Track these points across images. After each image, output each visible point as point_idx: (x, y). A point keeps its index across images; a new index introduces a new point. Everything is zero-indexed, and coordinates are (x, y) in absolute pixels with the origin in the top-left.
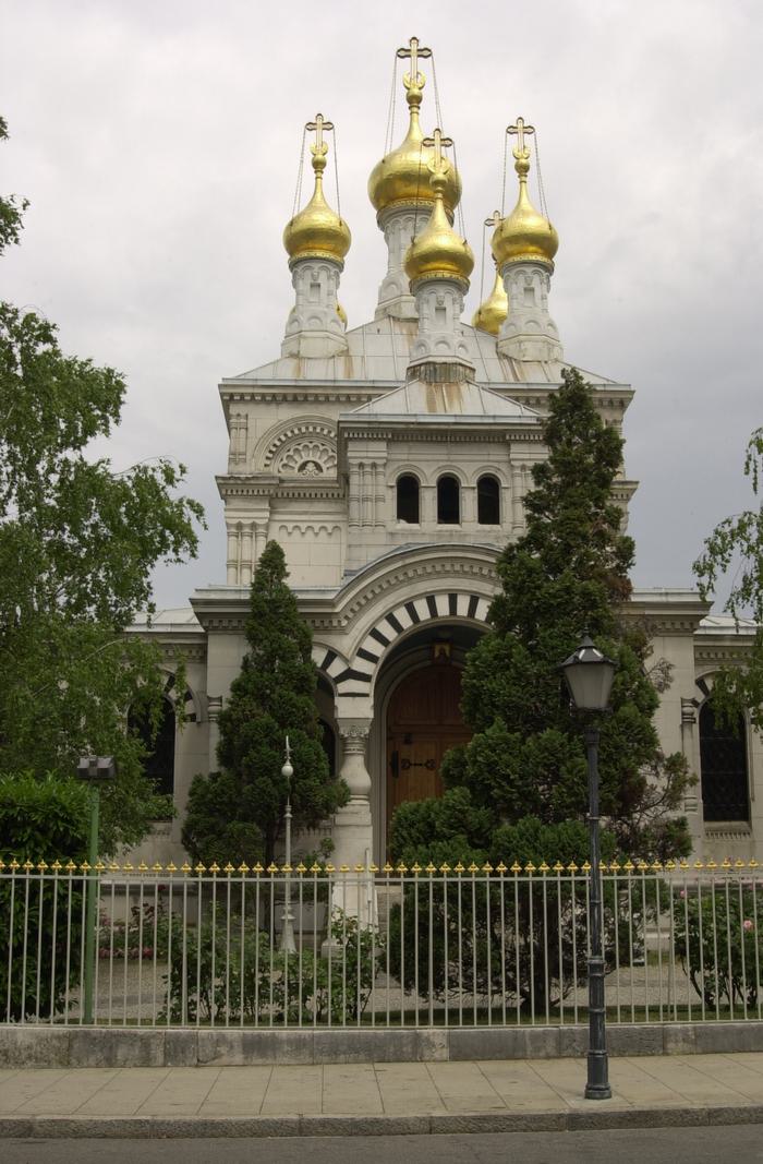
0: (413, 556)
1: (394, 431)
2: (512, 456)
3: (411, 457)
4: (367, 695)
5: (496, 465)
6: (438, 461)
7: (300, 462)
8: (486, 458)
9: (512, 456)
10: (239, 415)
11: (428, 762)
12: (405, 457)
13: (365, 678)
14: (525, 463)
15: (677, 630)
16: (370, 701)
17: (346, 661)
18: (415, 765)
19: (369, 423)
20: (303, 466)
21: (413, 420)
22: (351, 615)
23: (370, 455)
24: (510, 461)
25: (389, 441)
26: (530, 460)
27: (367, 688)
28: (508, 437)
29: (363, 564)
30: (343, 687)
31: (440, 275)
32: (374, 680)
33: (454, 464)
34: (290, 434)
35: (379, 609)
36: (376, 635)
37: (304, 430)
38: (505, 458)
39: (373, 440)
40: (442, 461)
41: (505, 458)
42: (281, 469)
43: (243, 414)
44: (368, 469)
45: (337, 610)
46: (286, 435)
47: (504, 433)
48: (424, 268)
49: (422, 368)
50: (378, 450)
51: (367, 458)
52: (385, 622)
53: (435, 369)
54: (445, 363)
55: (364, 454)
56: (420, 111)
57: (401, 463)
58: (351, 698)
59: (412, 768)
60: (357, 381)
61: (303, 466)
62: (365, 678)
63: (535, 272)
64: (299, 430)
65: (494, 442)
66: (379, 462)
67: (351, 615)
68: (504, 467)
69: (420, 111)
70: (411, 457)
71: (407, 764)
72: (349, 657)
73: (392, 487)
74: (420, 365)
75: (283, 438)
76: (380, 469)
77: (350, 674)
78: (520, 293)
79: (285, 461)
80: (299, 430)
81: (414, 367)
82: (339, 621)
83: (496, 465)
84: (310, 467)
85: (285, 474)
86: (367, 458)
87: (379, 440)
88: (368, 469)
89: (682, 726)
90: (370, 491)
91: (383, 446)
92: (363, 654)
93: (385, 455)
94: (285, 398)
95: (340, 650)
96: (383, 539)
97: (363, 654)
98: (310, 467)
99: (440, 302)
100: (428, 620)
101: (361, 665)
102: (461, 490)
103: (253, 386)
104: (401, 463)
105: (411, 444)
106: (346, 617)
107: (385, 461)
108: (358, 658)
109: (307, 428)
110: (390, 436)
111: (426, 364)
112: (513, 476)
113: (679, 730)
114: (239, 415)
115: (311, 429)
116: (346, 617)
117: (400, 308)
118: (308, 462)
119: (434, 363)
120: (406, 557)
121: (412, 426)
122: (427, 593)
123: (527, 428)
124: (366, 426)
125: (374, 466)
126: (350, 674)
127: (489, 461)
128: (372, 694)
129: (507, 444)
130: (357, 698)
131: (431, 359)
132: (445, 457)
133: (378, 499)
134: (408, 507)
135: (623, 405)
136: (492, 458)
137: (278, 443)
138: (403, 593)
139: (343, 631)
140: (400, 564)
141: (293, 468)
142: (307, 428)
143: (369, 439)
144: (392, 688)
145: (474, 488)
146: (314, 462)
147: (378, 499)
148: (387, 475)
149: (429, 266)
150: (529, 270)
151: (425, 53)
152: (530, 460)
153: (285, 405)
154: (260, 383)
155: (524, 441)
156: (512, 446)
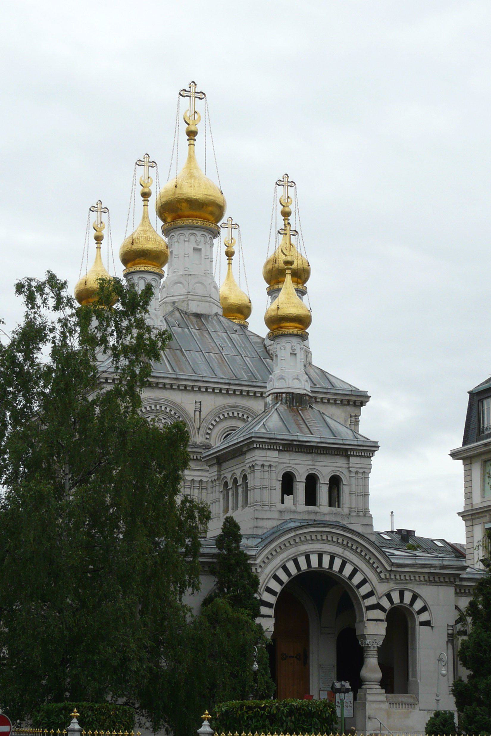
0: (301, 529)
1: (283, 445)
2: (351, 465)
3: (292, 462)
4: (270, 616)
6: (307, 465)
8: (334, 465)
9: (351, 465)
12: (288, 461)
13: (268, 605)
14: (358, 470)
15: (446, 582)
21: (296, 439)
22: (263, 565)
23: (269, 459)
24: (349, 468)
25: (279, 451)
26: (361, 468)
27: (270, 612)
28: (349, 453)
29: (265, 531)
31: (295, 332)
33: (316, 467)
35: (277, 561)
36: (276, 578)
37: (153, 407)
38: (346, 466)
39: (271, 449)
40: (307, 465)
41: (346, 466)
44: (266, 468)
45: (256, 563)
47: (346, 450)
48: (283, 325)
49: (284, 395)
50: (273, 456)
51: (267, 461)
55: (264, 459)
56: (195, 143)
57: (285, 465)
62: (268, 605)
64: (150, 407)
67: (263, 565)
68: (345, 471)
69: (195, 143)
70: (292, 462)
73: (279, 480)
74: (282, 393)
76: (273, 469)
80: (150, 407)
81: (277, 393)
82: (256, 569)
86: (267, 461)
87: (274, 450)
88: (266, 468)
89: (447, 642)
90: (267, 483)
91: (276, 453)
93: (277, 460)
96: (276, 515)
99: (293, 349)
100: (305, 570)
102: (318, 485)
104: (285, 465)
106: (260, 566)
108: (265, 593)
109: (156, 406)
111: (287, 393)
112: (350, 477)
113: (446, 643)
115: (158, 407)
116: (260, 566)
117: (188, 305)
119: (293, 393)
120: (297, 530)
122: (306, 552)
123: (362, 448)
124: (268, 441)
125: (270, 466)
127: (336, 467)
128: (273, 616)
129: (348, 457)
130: (265, 618)
132: (310, 463)
133: (272, 488)
135: (362, 404)
136: (338, 465)
138: (291, 552)
140: (293, 534)
142: (156, 406)
143: (268, 449)
145: (327, 484)
147: (272, 488)
152: (361, 468)
155: (357, 456)
156: (351, 458)
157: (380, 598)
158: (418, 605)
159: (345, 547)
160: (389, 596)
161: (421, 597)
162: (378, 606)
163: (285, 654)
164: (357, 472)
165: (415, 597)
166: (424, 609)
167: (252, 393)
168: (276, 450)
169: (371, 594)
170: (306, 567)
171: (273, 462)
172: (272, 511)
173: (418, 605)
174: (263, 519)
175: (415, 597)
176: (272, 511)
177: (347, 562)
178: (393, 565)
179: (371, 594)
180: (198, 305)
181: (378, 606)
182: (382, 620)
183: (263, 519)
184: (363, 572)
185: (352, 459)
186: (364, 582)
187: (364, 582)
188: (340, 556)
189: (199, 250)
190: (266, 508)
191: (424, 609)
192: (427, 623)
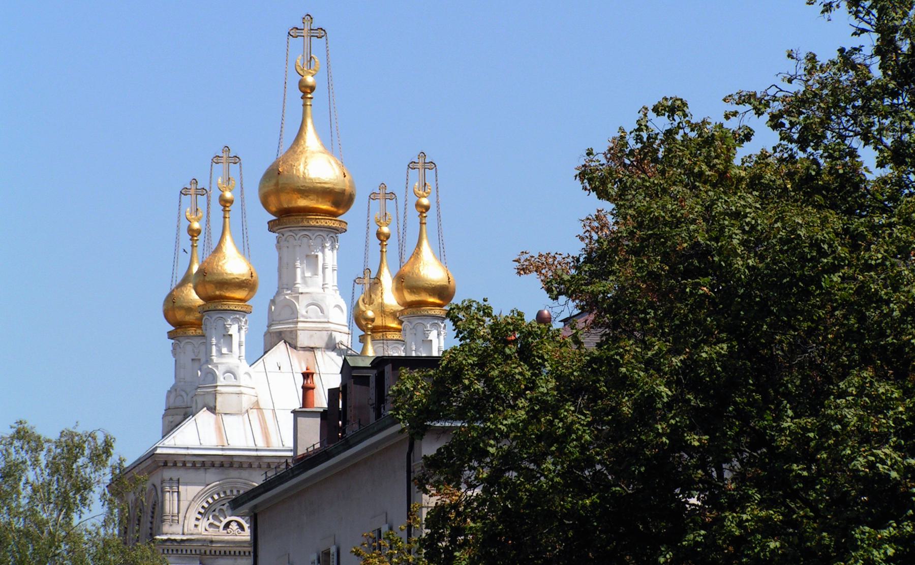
7: (225, 521)
10: (171, 479)
20: (227, 526)
34: (216, 497)
42: (207, 528)
43: (175, 478)
46: (212, 498)
60: (276, 450)
61: (227, 526)
75: (210, 501)
79: (211, 520)
84: (234, 526)
85: (212, 534)
94: (213, 465)
98: (234, 526)
114: (171, 479)
118: (232, 521)
137: (206, 505)
141: (218, 527)
146: (236, 521)
151: (320, 33)
153: (213, 470)
180: (311, 336)
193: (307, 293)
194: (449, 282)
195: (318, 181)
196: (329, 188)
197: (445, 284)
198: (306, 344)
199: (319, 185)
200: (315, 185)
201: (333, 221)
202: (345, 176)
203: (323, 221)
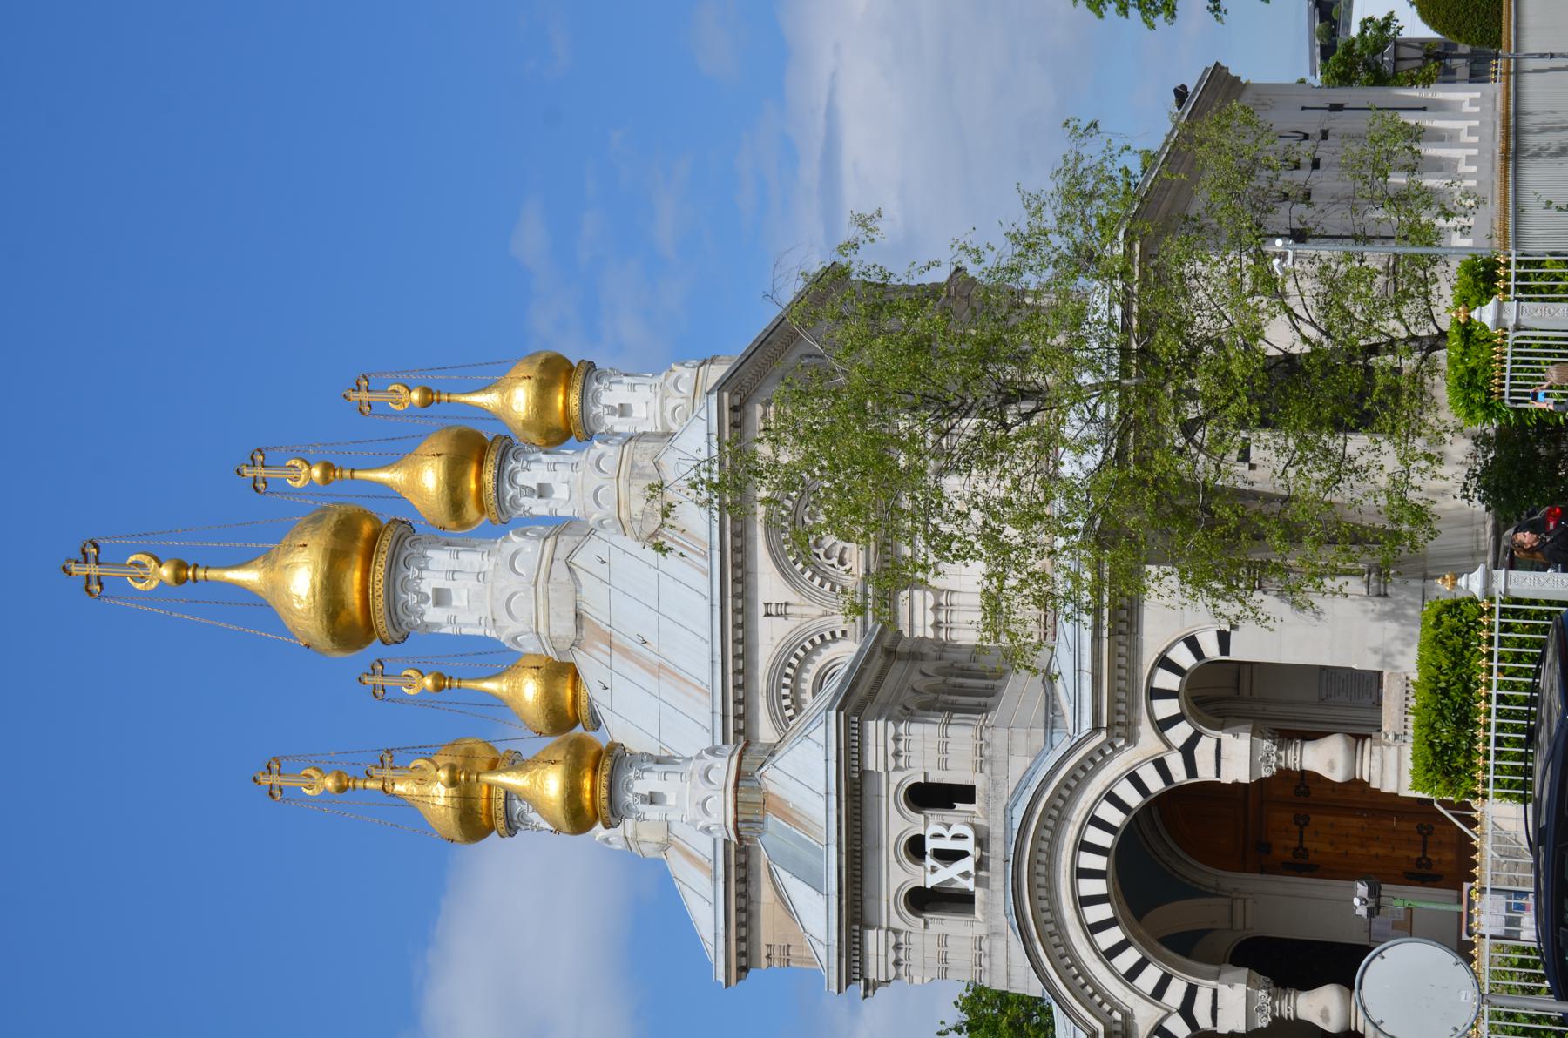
5: (893, 788)
11: (1297, 823)
13: (1191, 992)
16: (1223, 990)
17: (1169, 1013)
18: (1301, 840)
19: (840, 956)
23: (882, 952)
30: (1204, 1022)
32: (1194, 980)
47: (849, 780)
50: (875, 941)
51: (886, 956)
52: (1115, 961)
53: (745, 821)
54: (736, 807)
58: (1219, 1013)
59: (1306, 845)
62: (1191, 992)
63: (512, 481)
65: (861, 790)
66: (892, 941)
71: (1300, 851)
72: (1162, 1013)
73: (926, 924)
77: (1186, 1011)
78: (547, 504)
83: (893, 788)
86: (886, 956)
91: (871, 935)
92: (1159, 991)
93: (882, 933)
95: (1155, 1021)
97: (1159, 991)
100: (1113, 908)
101: (1175, 994)
103: (727, 940)
105: (865, 894)
107: (890, 933)
110: (857, 927)
119: (736, 821)
121: (844, 902)
122: (1076, 907)
126: (1186, 1011)
129: (863, 773)
130: (1219, 1006)
131: (731, 825)
134: (955, 901)
139: (1128, 1016)
144: (1190, 860)
148: (909, 929)
149: (587, 803)
150: (510, 492)
154: (721, 931)
157: (1169, 746)
158: (1184, 657)
159: (1060, 926)
160: (1163, 726)
161: (1167, 649)
162: (1188, 751)
163: (1297, 787)
164: (897, 754)
165: (1164, 662)
166: (1192, 643)
167: (737, 664)
168: (861, 937)
169: (1161, 766)
170: (1105, 859)
171: (887, 941)
172: (990, 951)
173: (1184, 657)
174: (1008, 974)
175: (1164, 662)
176: (990, 951)
177: (1093, 815)
178: (1096, 728)
179: (1161, 766)
181: (1188, 751)
182: (1219, 742)
183: (1008, 974)
184: (1114, 782)
185: (871, 766)
186: (1134, 779)
187: (1134, 779)
188: (1081, 831)
189: (437, 591)
190: (985, 962)
191: (1192, 643)
192: (1224, 640)
193: (492, 613)
194: (439, 455)
195: (312, 600)
196: (322, 582)
197: (441, 463)
198: (572, 624)
199: (317, 598)
200: (318, 604)
201: (378, 567)
202: (305, 545)
203: (376, 586)
